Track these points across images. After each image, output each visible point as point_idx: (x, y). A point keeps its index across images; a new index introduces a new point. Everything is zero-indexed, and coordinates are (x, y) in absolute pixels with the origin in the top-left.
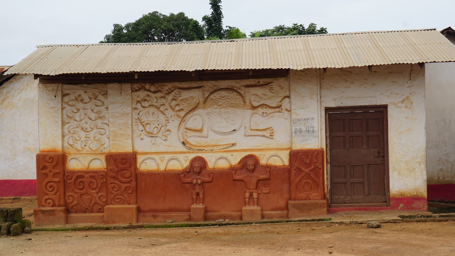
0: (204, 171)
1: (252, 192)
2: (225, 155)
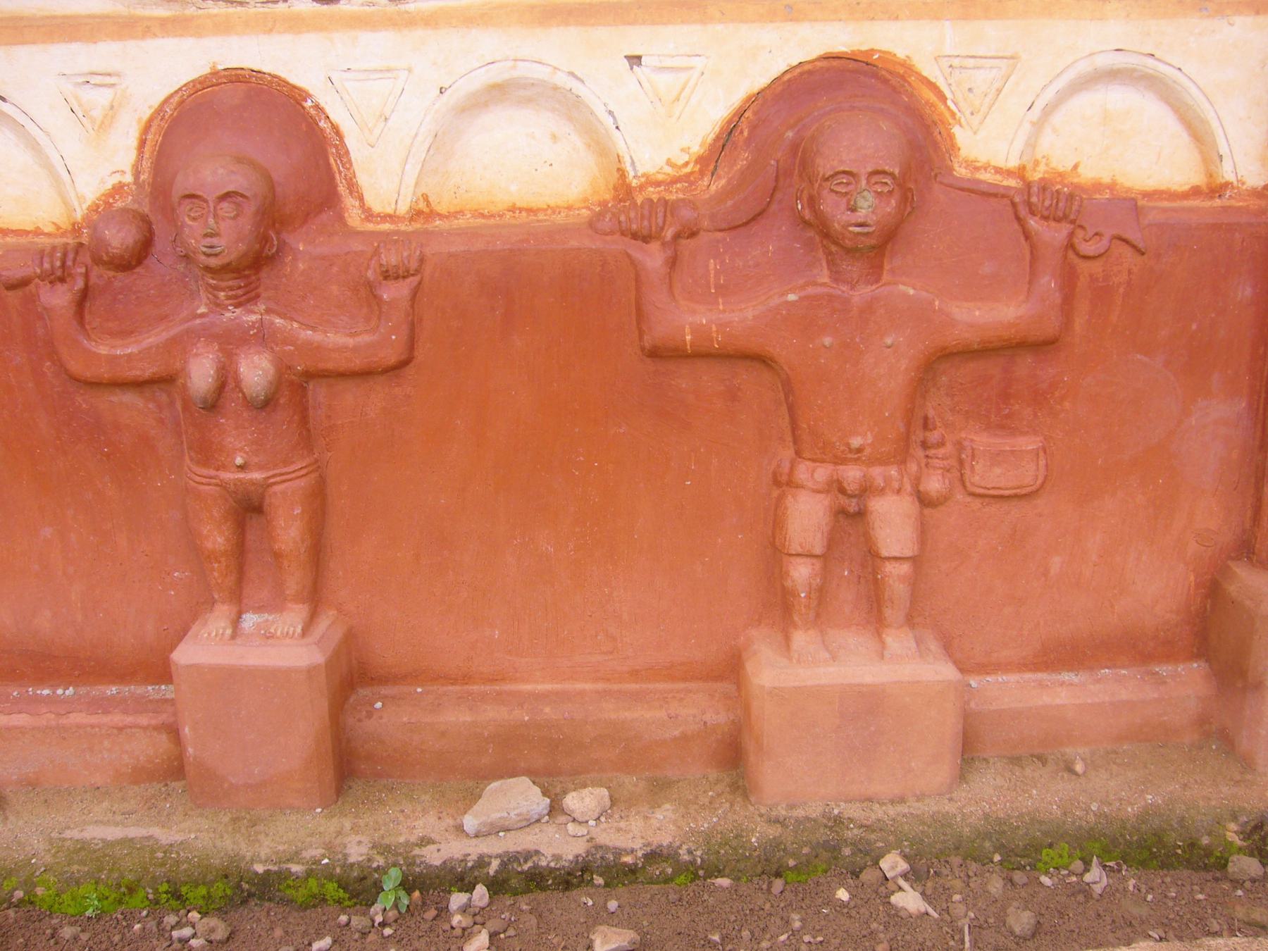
0: (305, 248)
1: (867, 490)
2: (553, 52)
